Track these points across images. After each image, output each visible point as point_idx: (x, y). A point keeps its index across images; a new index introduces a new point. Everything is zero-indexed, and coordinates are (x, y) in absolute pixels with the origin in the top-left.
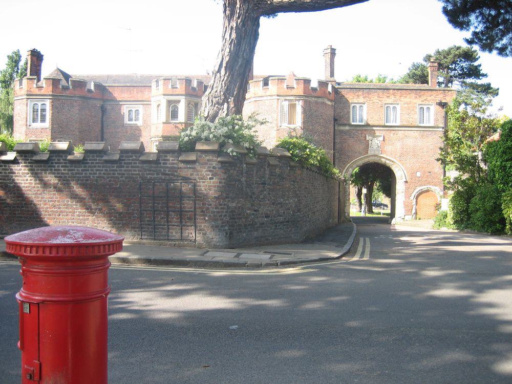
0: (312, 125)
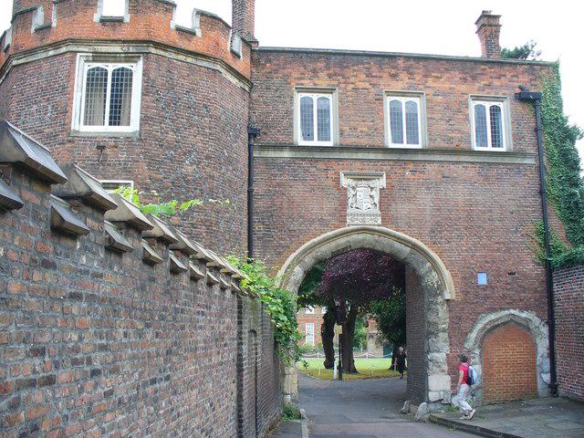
0: (177, 131)
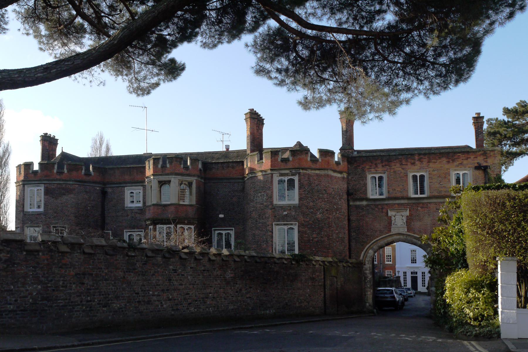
0: (313, 201)
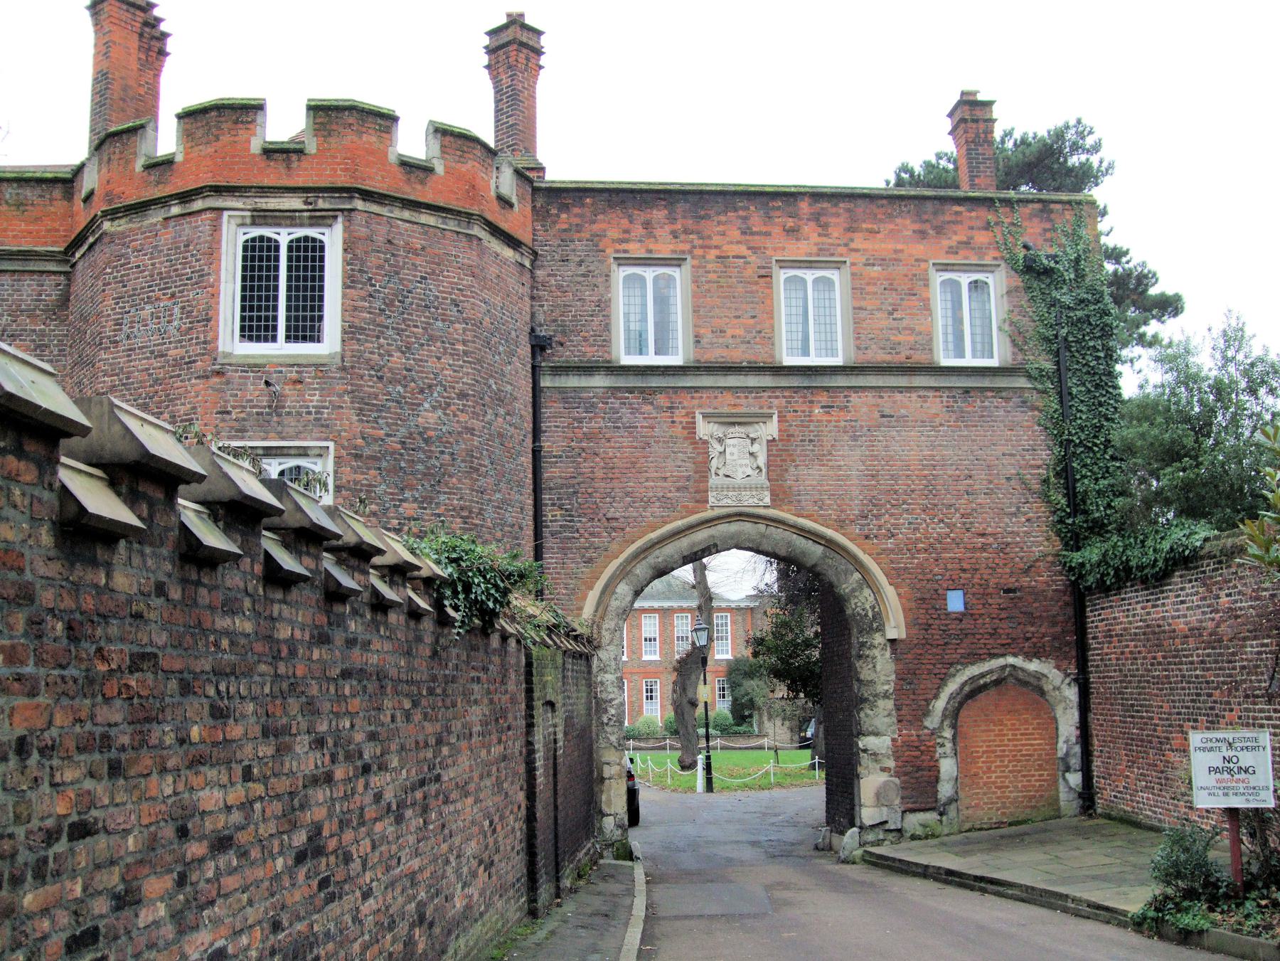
0: (407, 350)
